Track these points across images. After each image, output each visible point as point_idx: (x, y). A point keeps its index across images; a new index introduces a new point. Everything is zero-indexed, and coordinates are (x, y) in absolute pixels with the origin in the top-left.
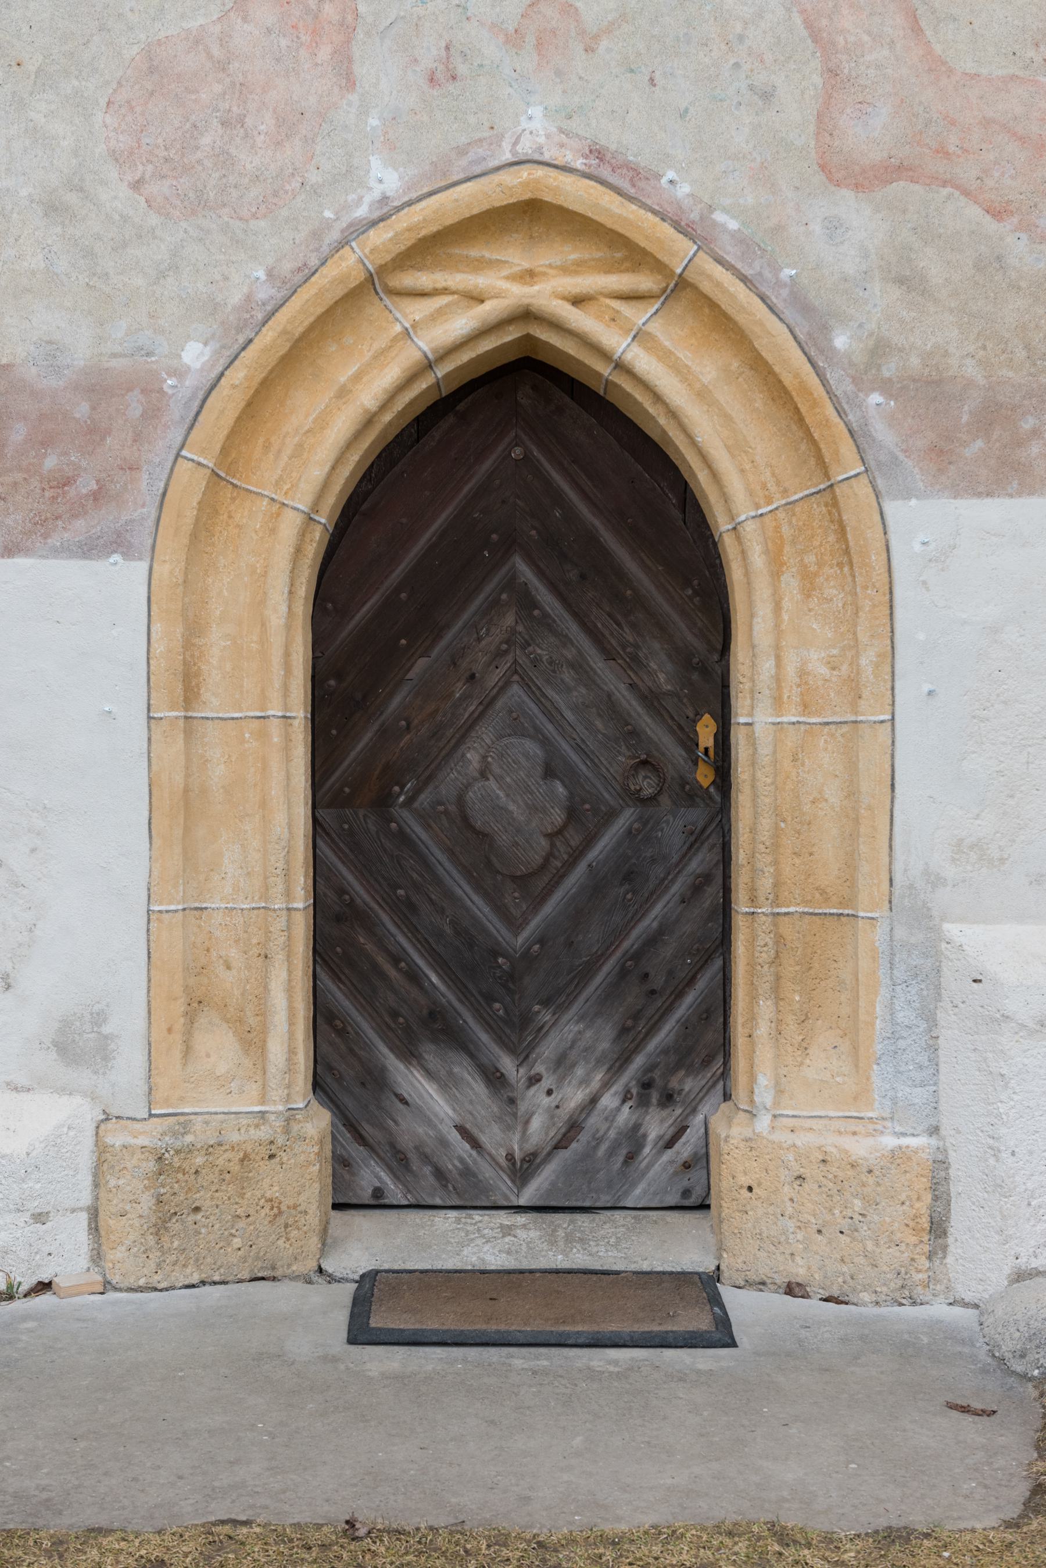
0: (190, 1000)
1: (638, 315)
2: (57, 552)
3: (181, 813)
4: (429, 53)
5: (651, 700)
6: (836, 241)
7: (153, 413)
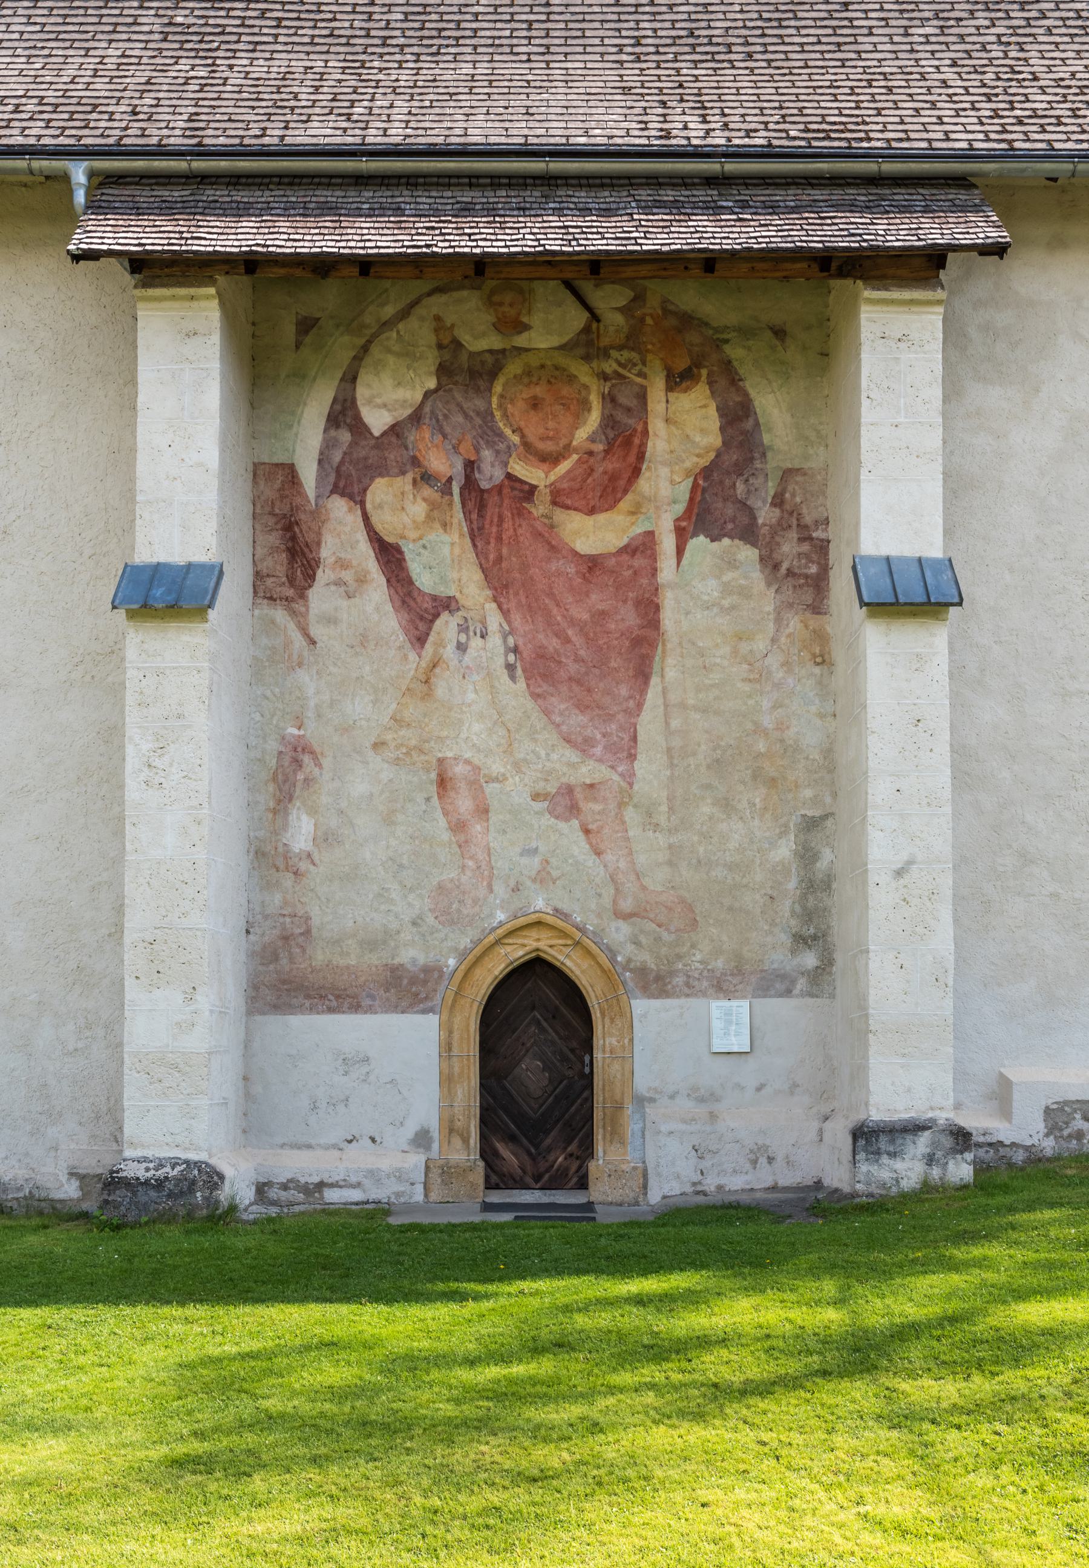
0: (450, 1129)
1: (567, 950)
2: (417, 1012)
3: (447, 1081)
4: (512, 883)
5: (572, 1050)
6: (618, 933)
7: (441, 976)
